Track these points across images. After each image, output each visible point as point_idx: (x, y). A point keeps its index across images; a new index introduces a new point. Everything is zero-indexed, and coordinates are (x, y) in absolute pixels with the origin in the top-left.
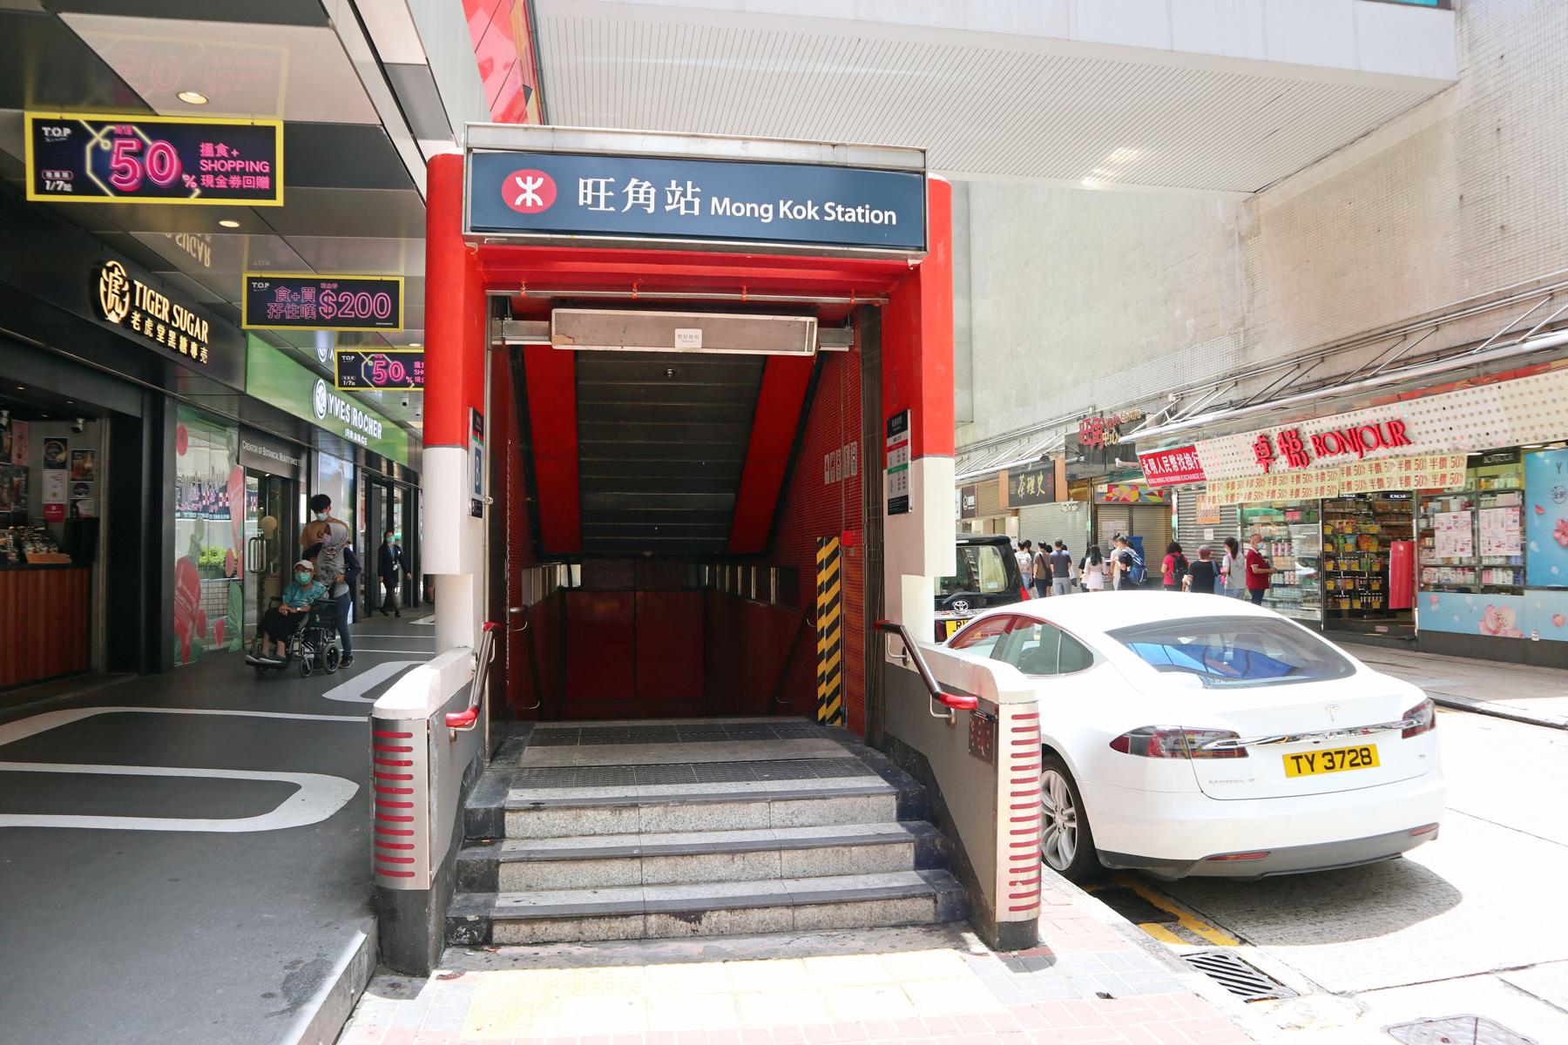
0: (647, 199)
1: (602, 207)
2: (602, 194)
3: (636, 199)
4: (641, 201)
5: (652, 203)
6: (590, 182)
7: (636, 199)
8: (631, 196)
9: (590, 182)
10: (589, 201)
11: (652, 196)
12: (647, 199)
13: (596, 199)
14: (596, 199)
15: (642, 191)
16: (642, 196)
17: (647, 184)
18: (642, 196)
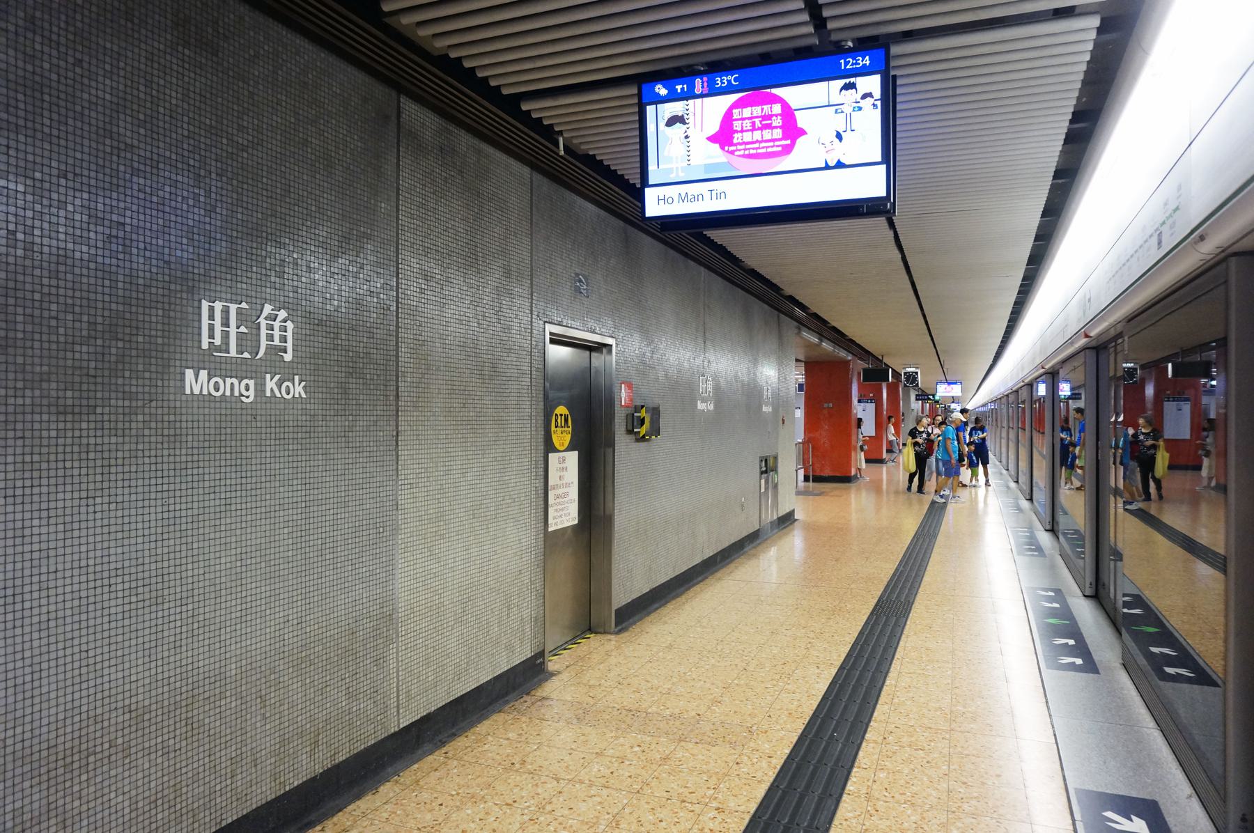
0: (283, 339)
1: (233, 352)
2: (233, 330)
3: (270, 337)
4: (277, 342)
5: (289, 345)
6: (218, 306)
7: (270, 337)
8: (264, 332)
9: (218, 306)
10: (218, 341)
11: (289, 335)
12: (283, 339)
13: (226, 335)
14: (226, 335)
15: (277, 324)
16: (277, 333)
17: (283, 314)
18: (277, 333)
